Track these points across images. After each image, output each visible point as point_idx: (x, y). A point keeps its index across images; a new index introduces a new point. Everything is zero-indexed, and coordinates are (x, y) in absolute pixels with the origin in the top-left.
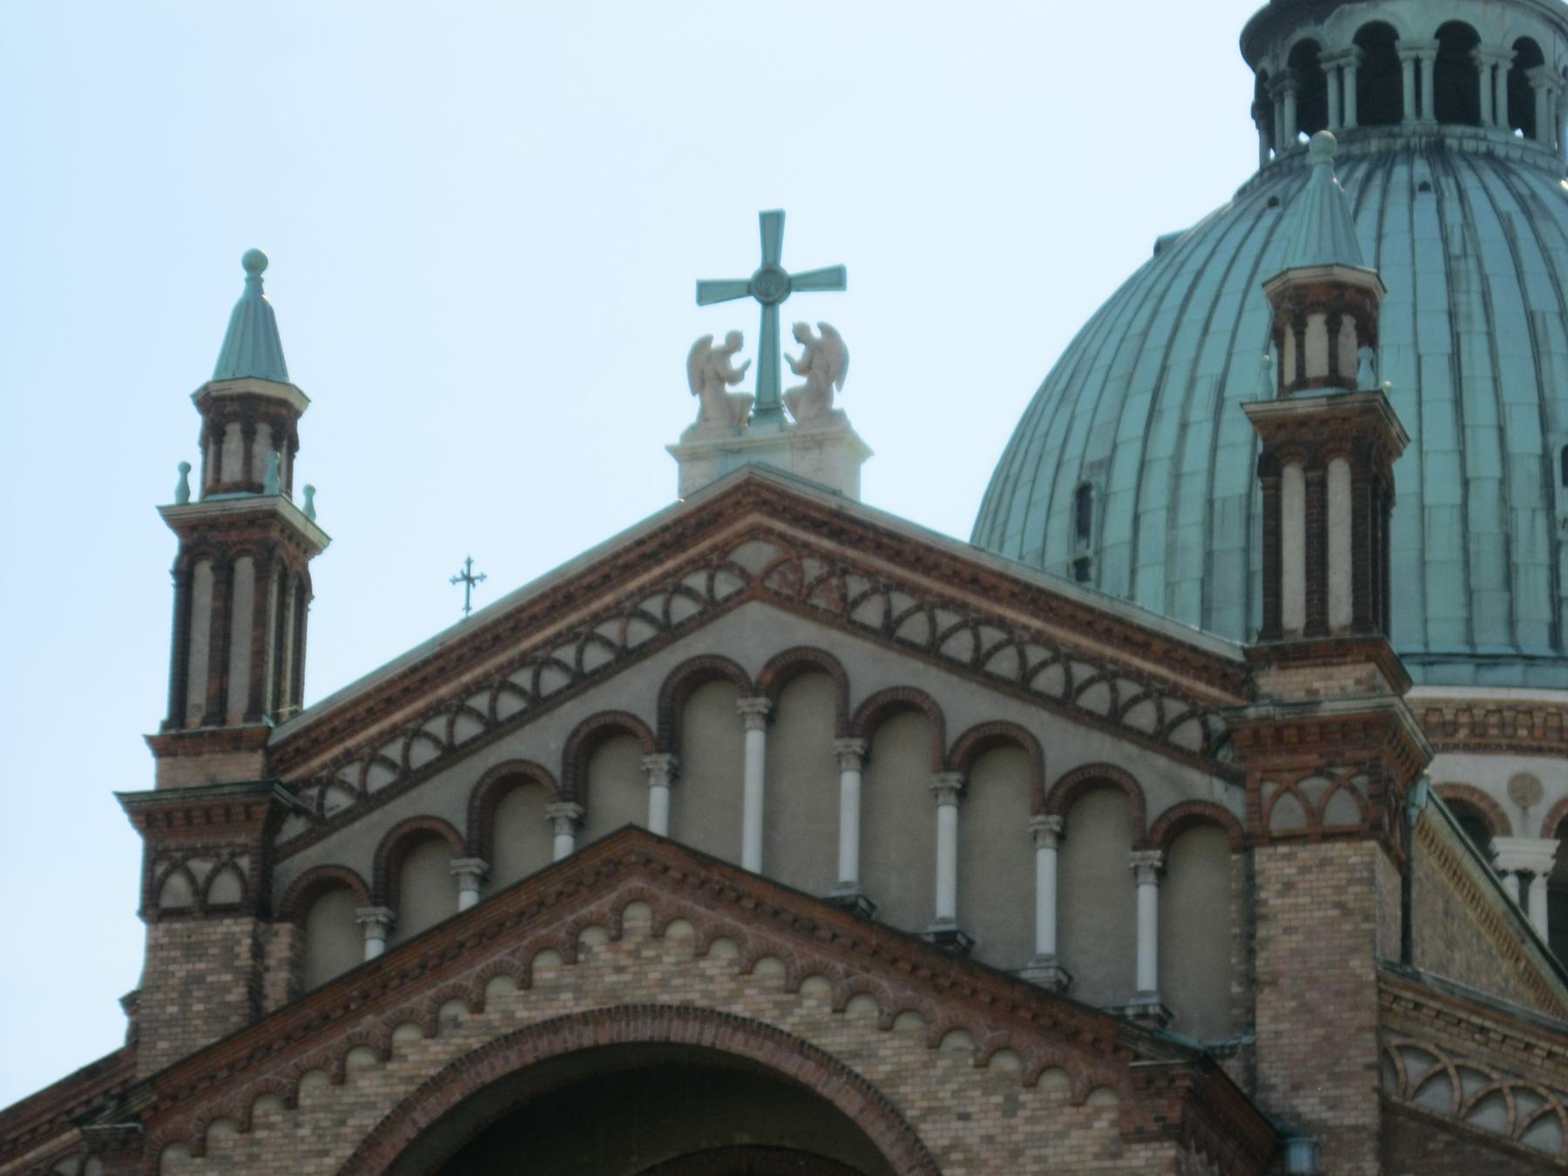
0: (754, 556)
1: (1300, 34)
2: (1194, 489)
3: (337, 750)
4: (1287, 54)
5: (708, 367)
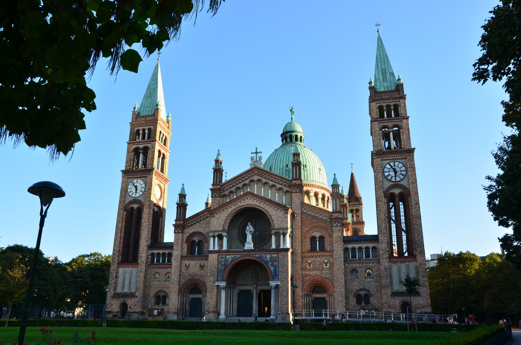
0: (256, 172)
2: (279, 168)
5: (252, 159)
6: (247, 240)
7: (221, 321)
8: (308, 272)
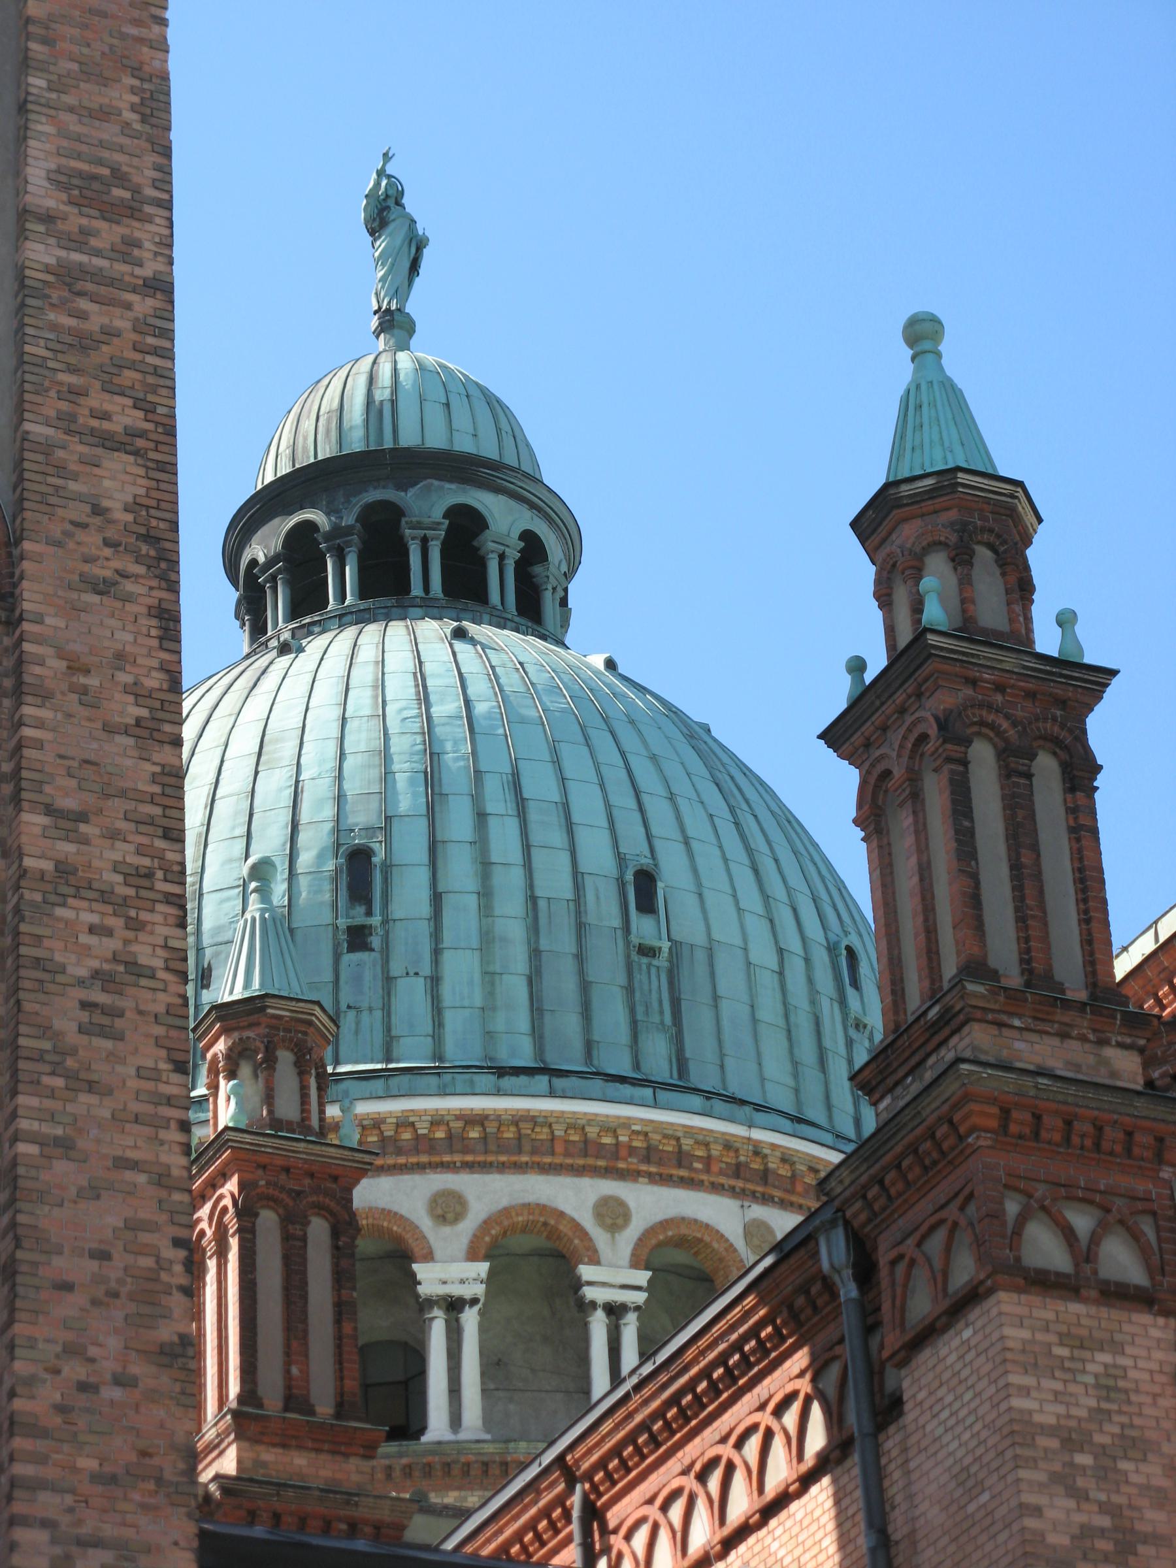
1: (374, 495)
4: (356, 510)
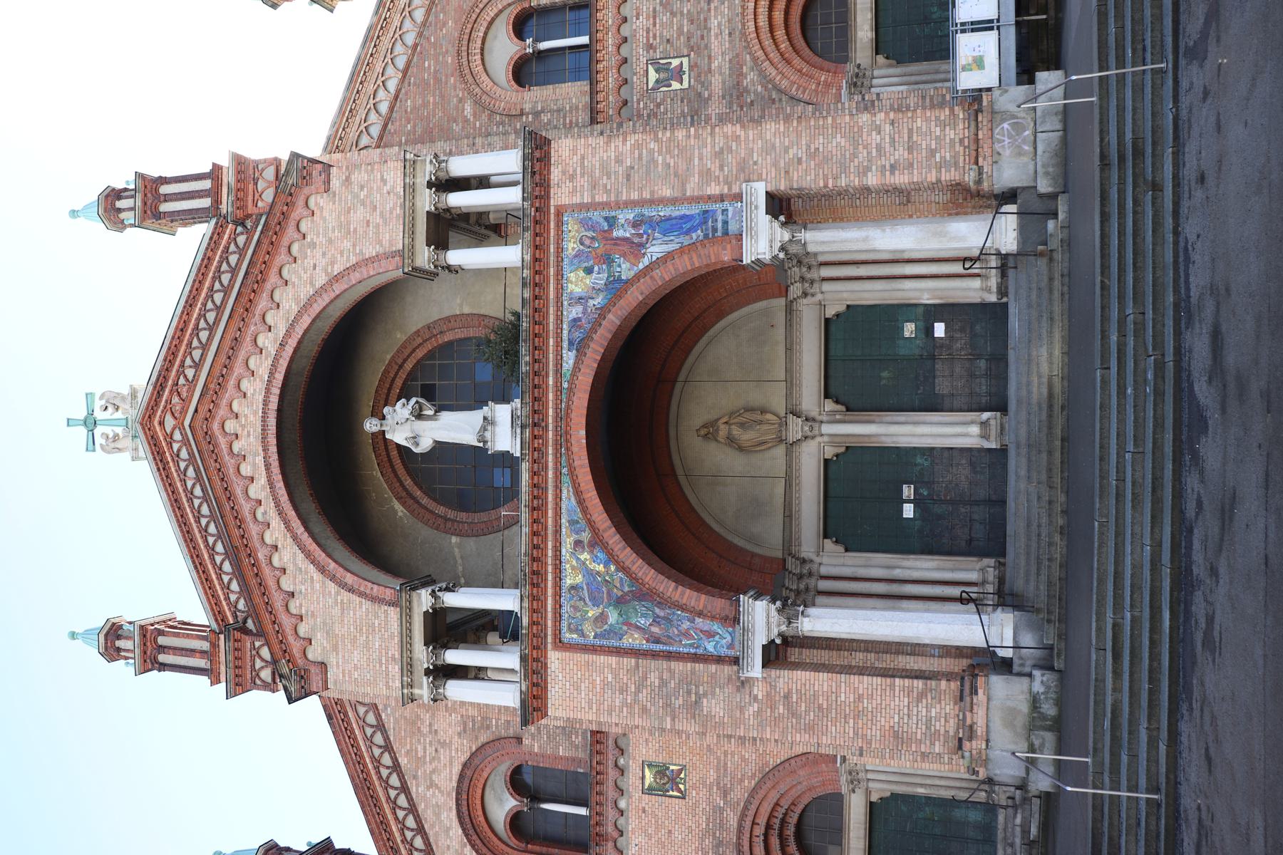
0: (170, 422)
3: (224, 603)
6: (470, 439)
7: (1028, 639)
8: (716, 82)
